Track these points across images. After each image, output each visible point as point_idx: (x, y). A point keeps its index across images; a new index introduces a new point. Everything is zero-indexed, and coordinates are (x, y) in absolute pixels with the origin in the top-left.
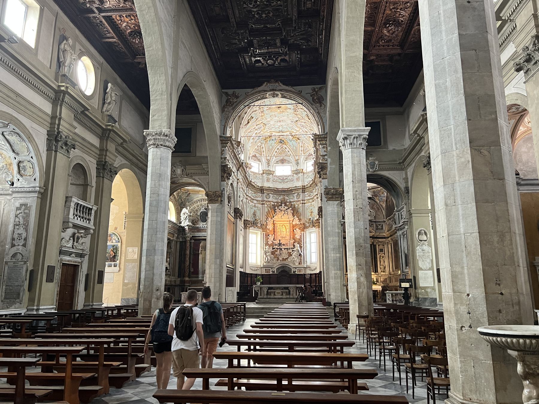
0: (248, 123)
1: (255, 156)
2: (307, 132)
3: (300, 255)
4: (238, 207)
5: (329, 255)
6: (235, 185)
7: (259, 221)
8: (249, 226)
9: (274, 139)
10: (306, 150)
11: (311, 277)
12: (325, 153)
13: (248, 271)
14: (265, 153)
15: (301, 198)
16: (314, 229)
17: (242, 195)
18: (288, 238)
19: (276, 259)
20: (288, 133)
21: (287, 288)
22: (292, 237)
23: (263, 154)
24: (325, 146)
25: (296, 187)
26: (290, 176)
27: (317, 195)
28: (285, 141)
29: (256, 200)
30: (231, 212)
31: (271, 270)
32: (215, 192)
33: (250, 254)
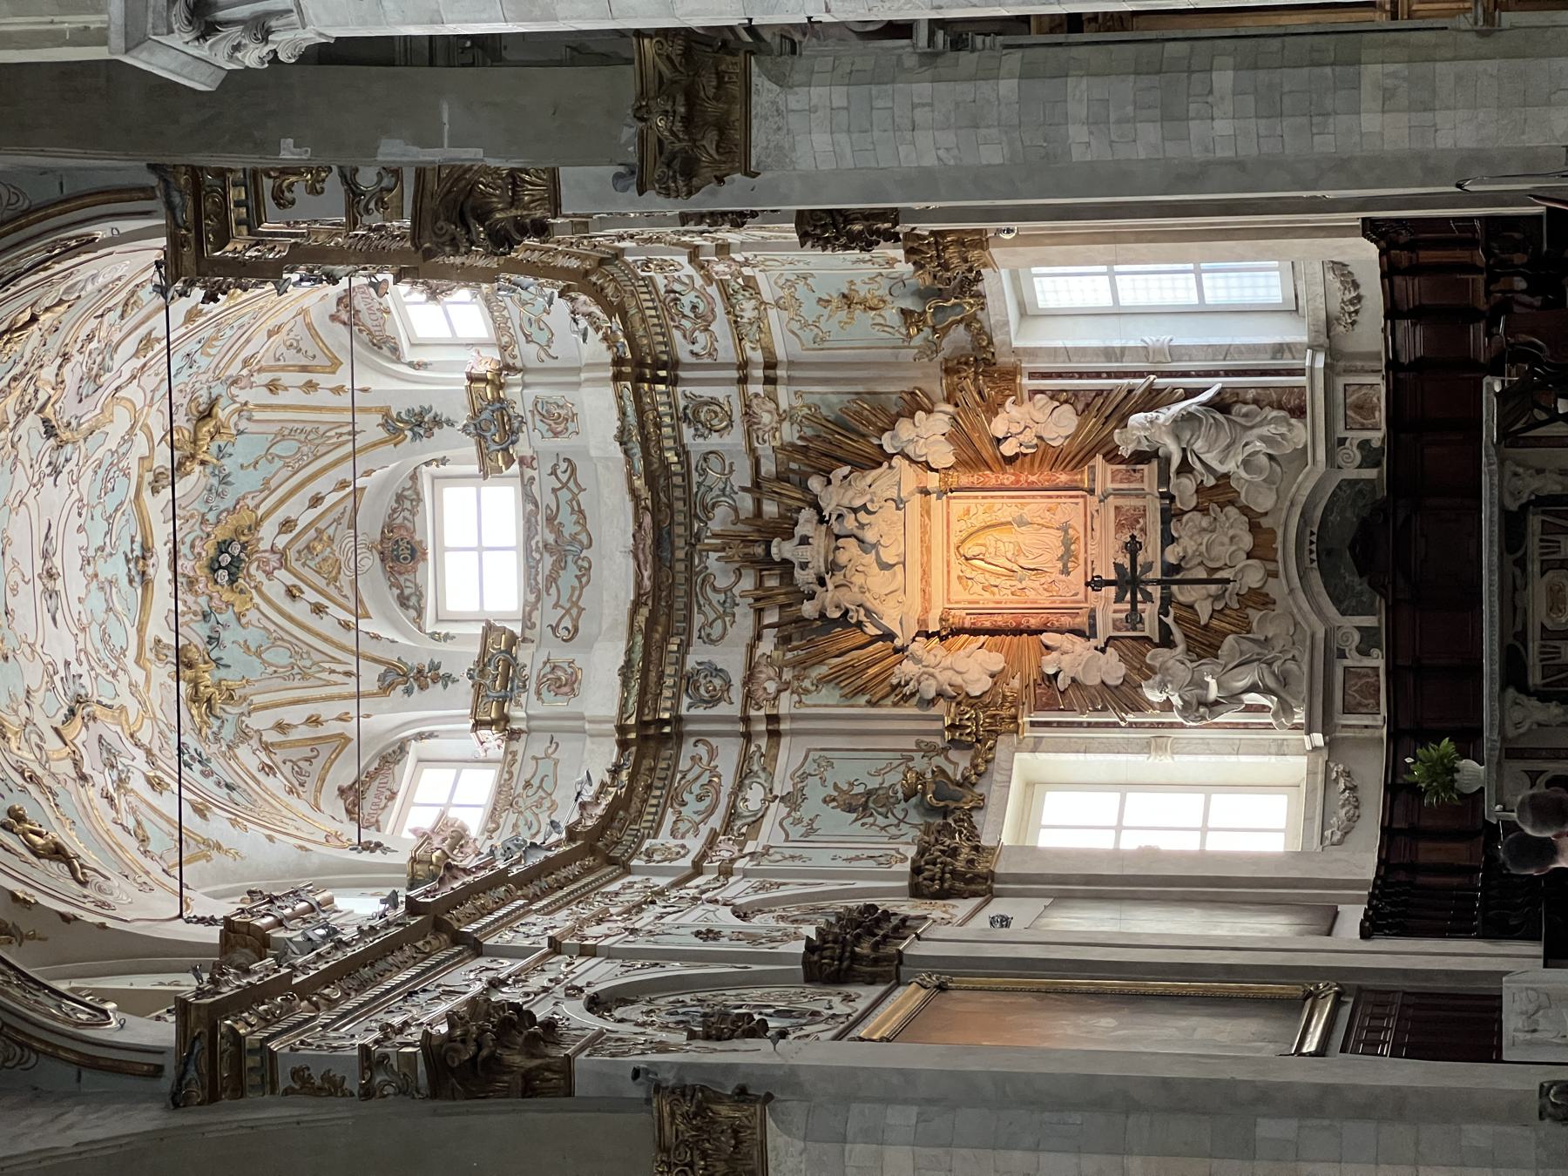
0: (58, 853)
1: (353, 796)
2: (147, 342)
3: (1221, 404)
4: (799, 947)
5: (1224, 152)
6: (600, 975)
7: (919, 763)
8: (965, 853)
9: (203, 630)
10: (307, 344)
11: (1418, 314)
12: (333, 183)
13: (1362, 861)
14: (328, 711)
15: (719, 393)
16: (997, 283)
17: (695, 917)
18: (1070, 510)
19: (1255, 615)
20: (156, 505)
21: (1513, 525)
22: (1063, 478)
23: (335, 728)
24: (267, 184)
25: (622, 438)
26: (527, 485)
27: (694, 253)
28: (220, 534)
29: (740, 786)
30: (840, 1008)
31: (1353, 661)
32: (663, 1148)
33: (1218, 843)
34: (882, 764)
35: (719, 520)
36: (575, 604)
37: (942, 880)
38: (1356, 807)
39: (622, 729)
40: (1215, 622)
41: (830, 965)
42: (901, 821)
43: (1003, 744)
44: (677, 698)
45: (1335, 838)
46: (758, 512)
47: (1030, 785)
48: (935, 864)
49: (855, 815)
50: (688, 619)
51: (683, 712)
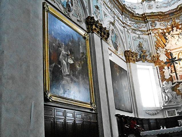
29: (140, 31)
31: (176, 112)
34: (147, 49)
35: (177, 21)
36: (161, 7)
37: (127, 55)
38: (153, 115)
39: (144, 14)
40: (178, 90)
41: (89, 20)
42: (138, 52)
43: (153, 64)
44: (151, 21)
45: (147, 112)
46: (179, 25)
47: (148, 69)
49: (138, 45)
50: (163, 21)
51: (149, 22)
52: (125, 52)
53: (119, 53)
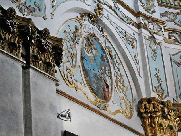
37: (146, 112)
48: (154, 108)
52: (141, 102)
53: (112, 107)
